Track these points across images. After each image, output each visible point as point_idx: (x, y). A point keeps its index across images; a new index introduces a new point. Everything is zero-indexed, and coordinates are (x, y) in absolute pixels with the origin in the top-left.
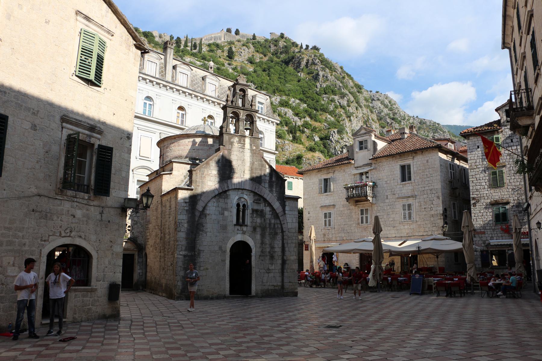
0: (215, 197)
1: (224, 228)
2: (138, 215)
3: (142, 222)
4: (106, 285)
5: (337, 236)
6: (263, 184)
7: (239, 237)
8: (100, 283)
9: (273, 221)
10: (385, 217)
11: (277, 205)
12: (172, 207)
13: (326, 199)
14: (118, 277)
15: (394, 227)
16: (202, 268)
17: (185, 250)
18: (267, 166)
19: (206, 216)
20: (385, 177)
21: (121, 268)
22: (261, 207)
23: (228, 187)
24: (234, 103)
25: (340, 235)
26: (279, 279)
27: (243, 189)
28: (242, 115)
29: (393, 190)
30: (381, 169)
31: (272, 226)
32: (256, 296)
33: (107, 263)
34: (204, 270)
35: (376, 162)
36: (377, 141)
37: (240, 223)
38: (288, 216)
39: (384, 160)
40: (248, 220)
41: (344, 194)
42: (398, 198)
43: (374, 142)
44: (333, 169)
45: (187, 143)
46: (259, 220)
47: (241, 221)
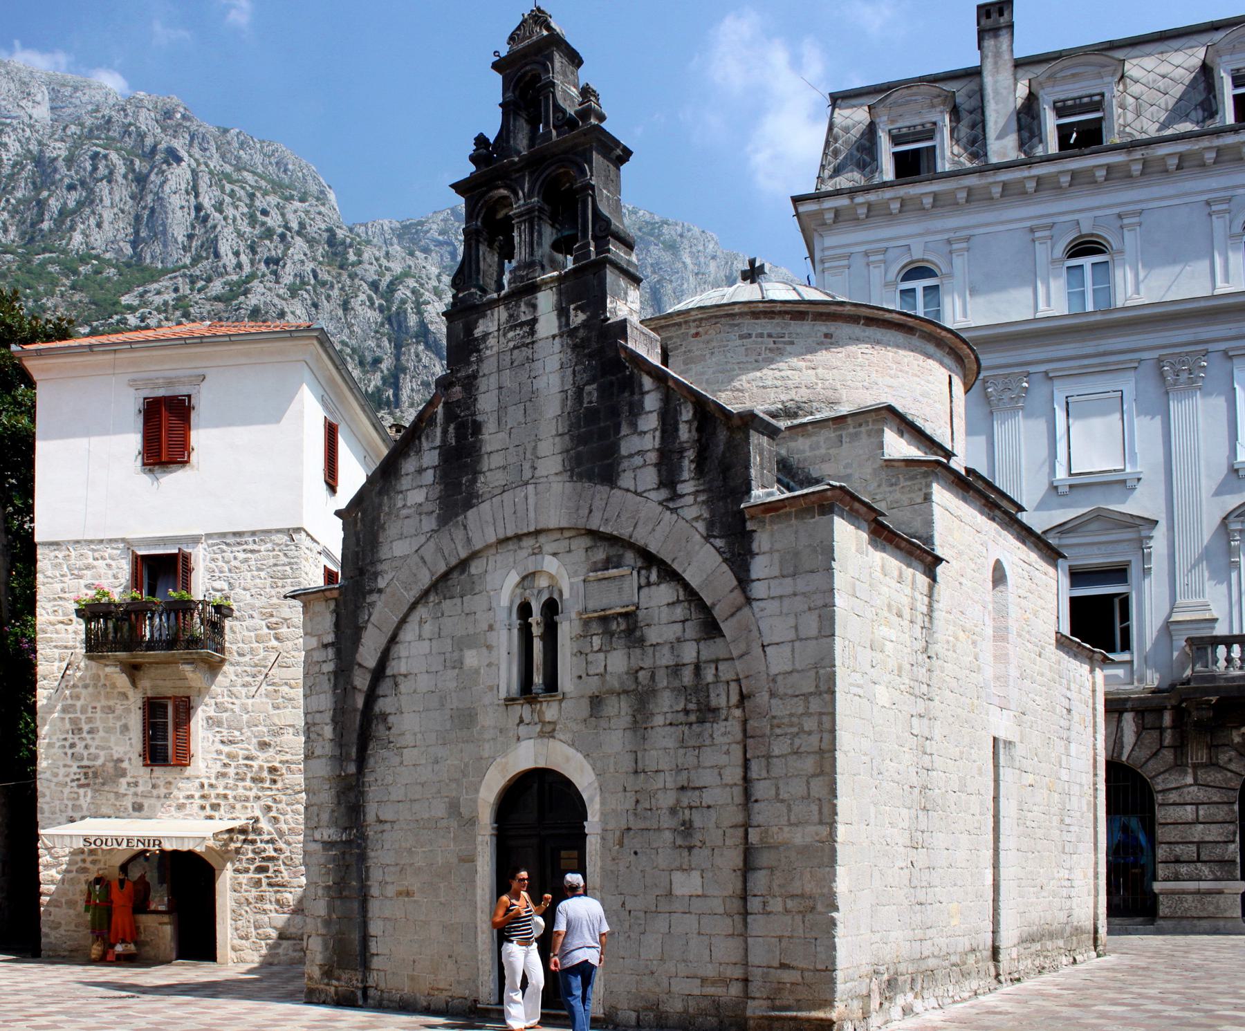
0: (425, 594)
6: (626, 480)
11: (703, 564)
17: (334, 823)
19: (396, 685)
23: (469, 540)
27: (537, 533)
31: (687, 676)
37: (536, 684)
38: (772, 607)
47: (538, 679)
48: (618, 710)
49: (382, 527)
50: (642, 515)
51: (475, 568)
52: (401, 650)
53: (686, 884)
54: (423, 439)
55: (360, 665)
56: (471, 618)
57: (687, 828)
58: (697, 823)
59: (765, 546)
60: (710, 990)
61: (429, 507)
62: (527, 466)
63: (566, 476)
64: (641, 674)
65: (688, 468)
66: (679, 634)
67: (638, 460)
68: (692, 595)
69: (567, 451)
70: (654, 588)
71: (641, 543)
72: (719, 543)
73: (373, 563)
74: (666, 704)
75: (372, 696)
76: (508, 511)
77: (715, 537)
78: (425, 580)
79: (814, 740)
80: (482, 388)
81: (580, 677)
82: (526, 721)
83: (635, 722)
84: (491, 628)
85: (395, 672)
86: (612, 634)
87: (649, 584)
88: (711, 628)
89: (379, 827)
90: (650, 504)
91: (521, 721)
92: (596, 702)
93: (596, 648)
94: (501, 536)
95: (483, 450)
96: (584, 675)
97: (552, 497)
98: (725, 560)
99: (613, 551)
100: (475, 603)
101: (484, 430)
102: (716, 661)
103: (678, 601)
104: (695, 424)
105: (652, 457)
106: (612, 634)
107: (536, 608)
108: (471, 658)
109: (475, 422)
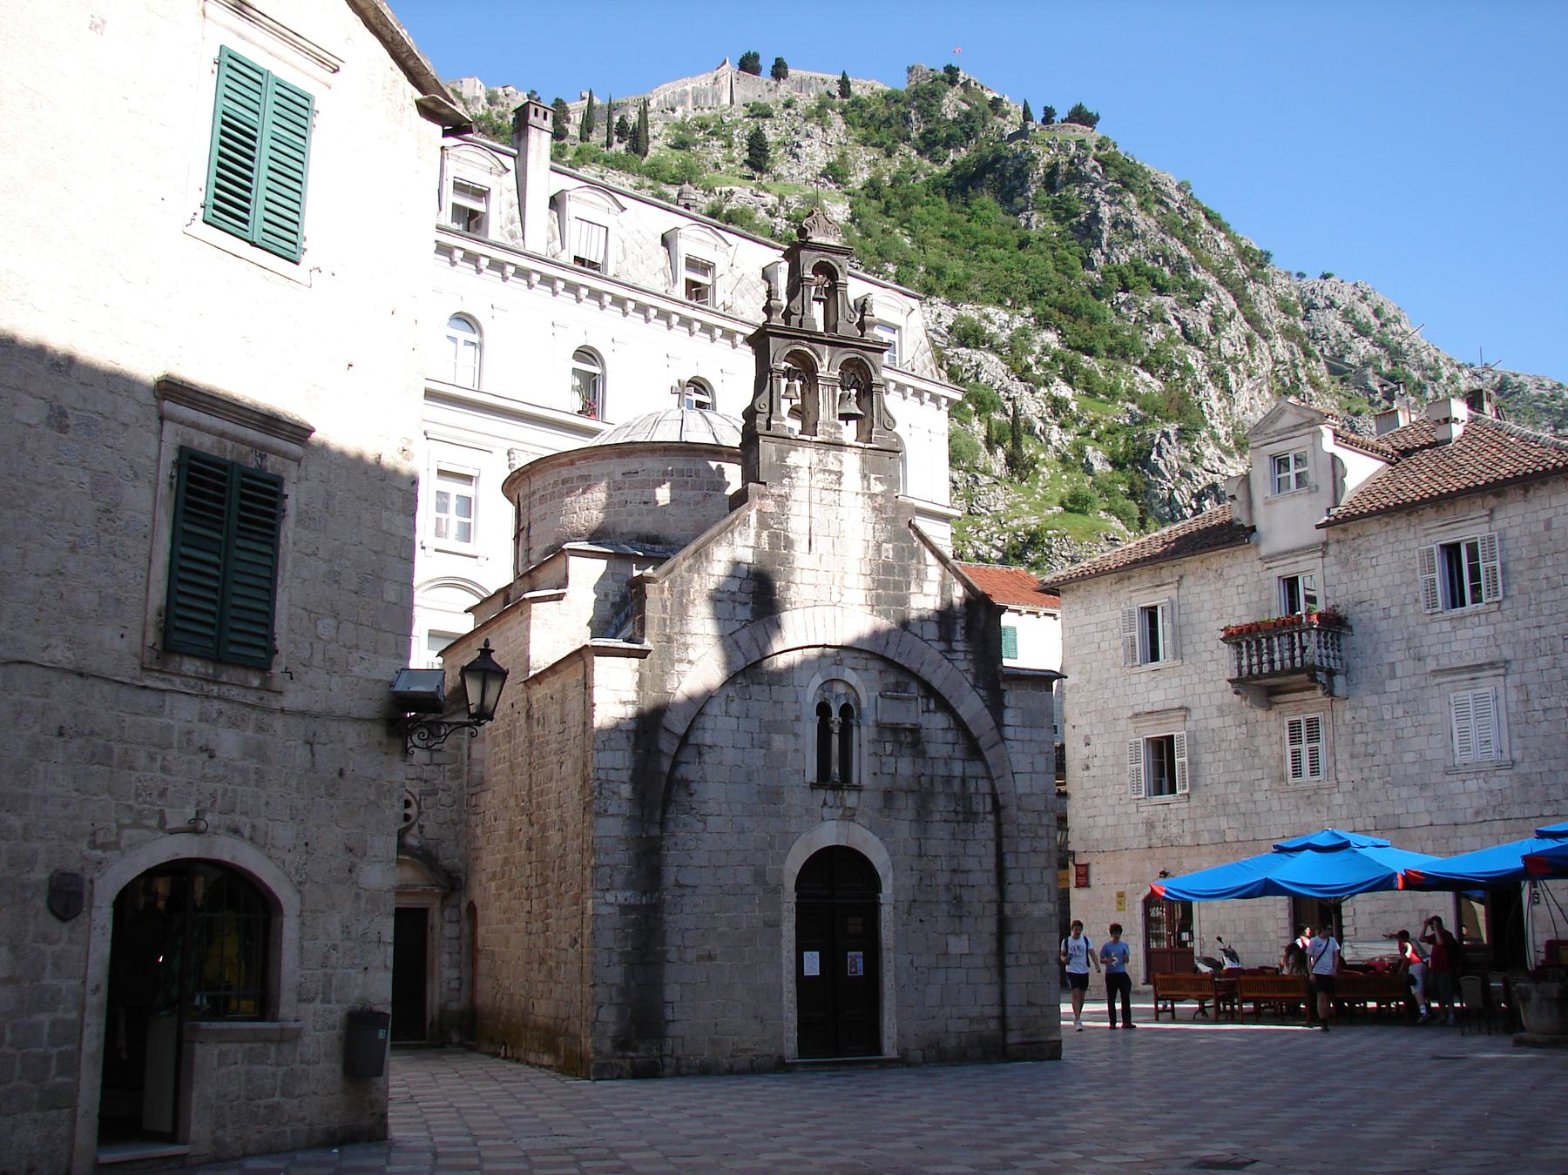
1: (772, 795)
2: (438, 758)
3: (454, 784)
4: (338, 1012)
5: (1200, 826)
7: (829, 834)
8: (311, 1006)
9: (958, 768)
10: (1387, 748)
11: (971, 705)
12: (569, 719)
13: (1155, 689)
14: (379, 989)
15: (1424, 787)
16: (690, 955)
18: (930, 558)
19: (700, 754)
20: (1382, 593)
21: (391, 949)
22: (911, 713)
24: (795, 320)
25: (1211, 823)
26: (989, 994)
28: (828, 364)
29: (1416, 642)
30: (1365, 563)
31: (957, 784)
32: (903, 1061)
33: (338, 931)
34: (700, 958)
35: (1342, 536)
36: (1342, 453)
37: (833, 775)
39: (1373, 527)
40: (863, 767)
41: (1223, 663)
42: (1436, 673)
43: (1333, 456)
44: (1178, 571)
45: (618, 477)
46: (905, 766)
47: (835, 769)
52: (708, 723)
53: (958, 945)
55: (667, 730)
56: (779, 706)
57: (958, 901)
58: (965, 898)
59: (1013, 703)
60: (976, 1027)
61: (742, 597)
62: (835, 590)
65: (959, 634)
72: (982, 692)
74: (941, 805)
75: (676, 763)
79: (1044, 842)
84: (798, 719)
85: (700, 741)
87: (928, 711)
88: (974, 751)
89: (678, 892)
91: (825, 804)
99: (901, 679)
102: (976, 778)
108: (778, 741)
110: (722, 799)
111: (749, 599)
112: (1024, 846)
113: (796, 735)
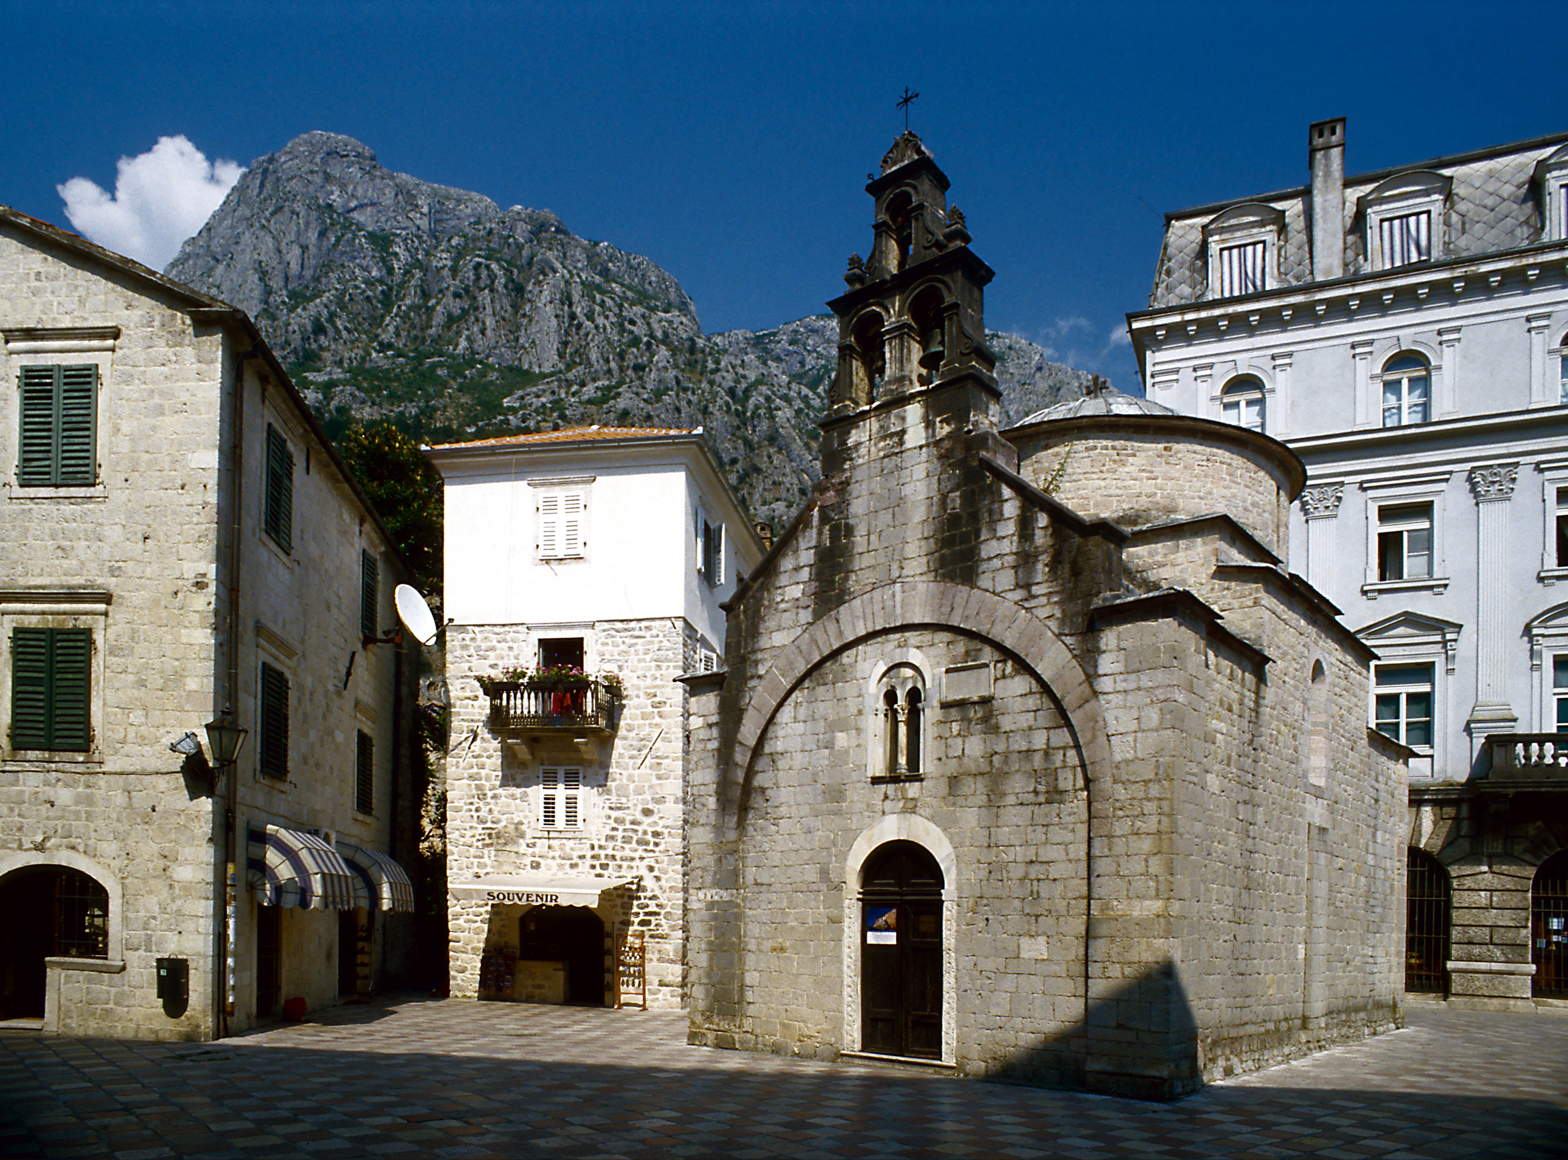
6: (985, 581)
48: (974, 790)
49: (762, 619)
50: (999, 613)
51: (846, 658)
54: (800, 540)
62: (895, 566)
63: (931, 576)
64: (995, 758)
65: (1041, 570)
66: (1031, 722)
67: (997, 563)
68: (1045, 688)
69: (932, 554)
70: (1008, 681)
71: (998, 639)
72: (1069, 640)
73: (754, 652)
76: (877, 607)
77: (1066, 635)
78: (802, 667)
80: (854, 494)
81: (940, 759)
82: (891, 797)
83: (990, 800)
84: (860, 712)
86: (970, 721)
87: (1004, 677)
90: (1007, 604)
92: (954, 781)
93: (955, 733)
94: (871, 630)
95: (855, 551)
96: (944, 758)
97: (917, 594)
98: (1075, 657)
100: (847, 689)
101: (856, 533)
103: (1031, 693)
104: (1050, 531)
105: (1010, 560)
106: (970, 721)
107: (901, 695)
108: (842, 739)
109: (847, 524)
110: (792, 802)
111: (810, 601)
112: (1121, 828)
113: (858, 729)
